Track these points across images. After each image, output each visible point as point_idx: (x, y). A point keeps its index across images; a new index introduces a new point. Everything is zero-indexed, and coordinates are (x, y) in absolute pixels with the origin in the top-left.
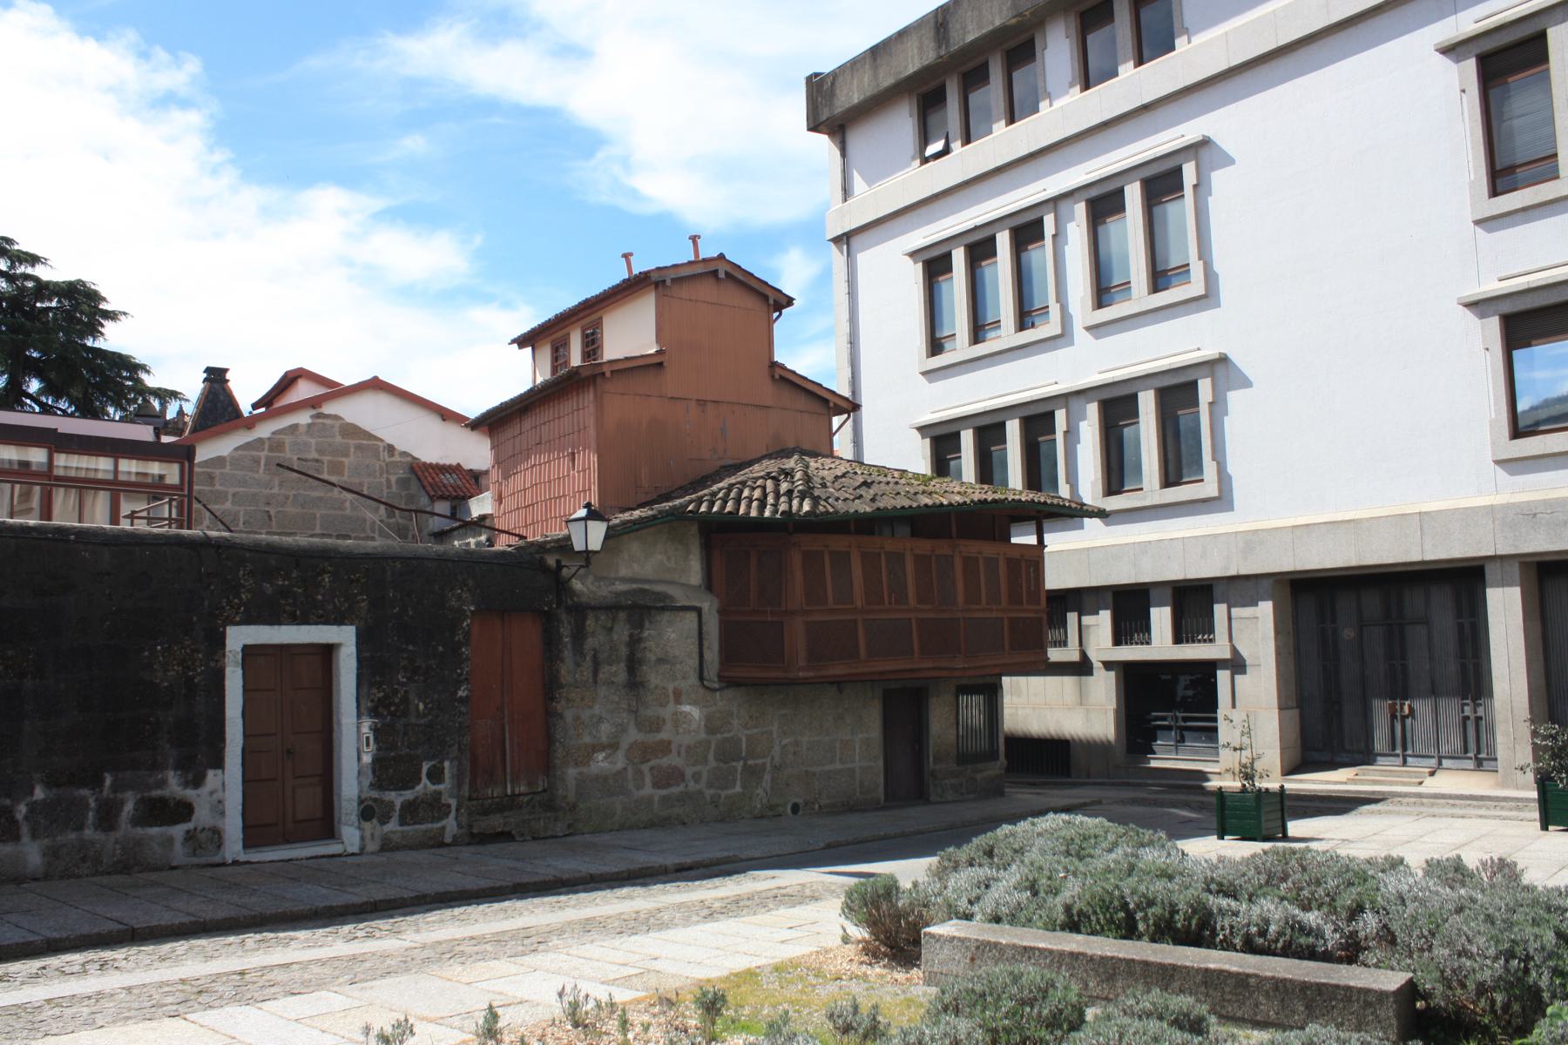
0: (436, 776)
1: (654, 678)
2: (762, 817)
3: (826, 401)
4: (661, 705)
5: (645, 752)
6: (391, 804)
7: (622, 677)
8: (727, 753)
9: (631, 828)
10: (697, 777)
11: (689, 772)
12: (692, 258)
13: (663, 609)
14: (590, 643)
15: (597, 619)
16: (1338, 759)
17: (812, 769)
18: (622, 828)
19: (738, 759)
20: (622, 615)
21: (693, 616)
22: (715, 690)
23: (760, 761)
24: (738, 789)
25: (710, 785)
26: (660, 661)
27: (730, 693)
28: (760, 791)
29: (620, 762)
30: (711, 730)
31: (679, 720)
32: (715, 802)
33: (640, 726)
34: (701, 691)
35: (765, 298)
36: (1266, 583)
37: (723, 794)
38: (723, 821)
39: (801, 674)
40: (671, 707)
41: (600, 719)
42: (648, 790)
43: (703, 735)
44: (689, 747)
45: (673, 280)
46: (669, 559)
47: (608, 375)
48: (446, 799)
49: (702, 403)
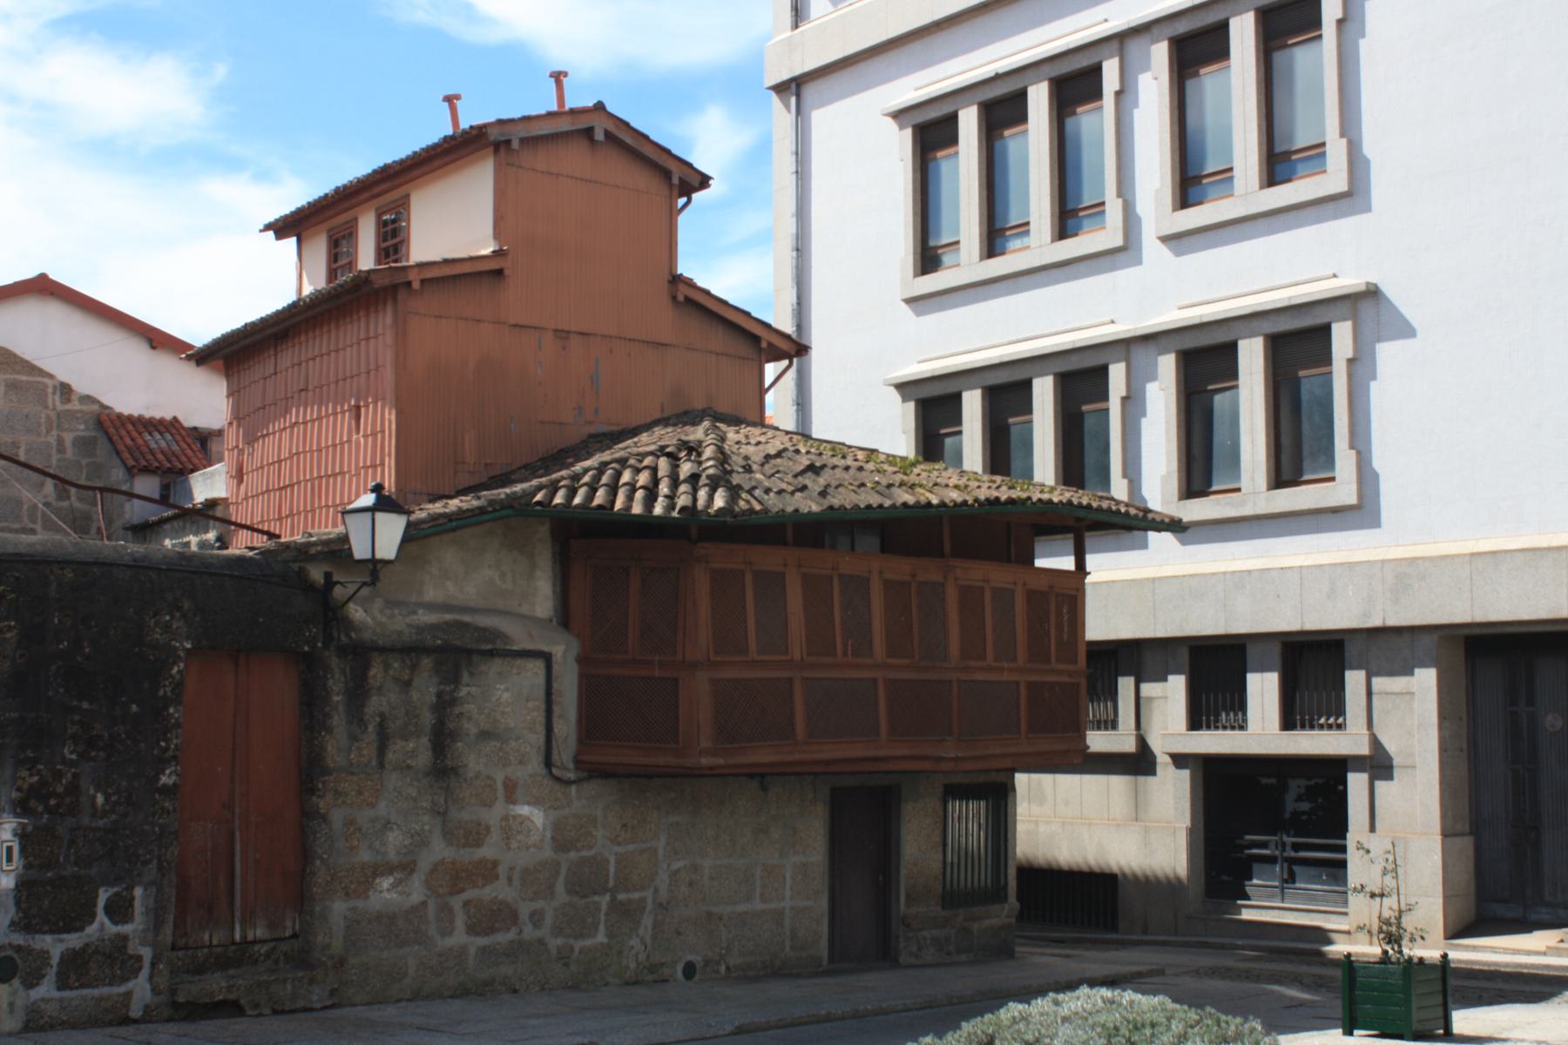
0: (119, 910)
1: (474, 761)
2: (636, 983)
3: (756, 339)
5: (456, 877)
6: (44, 956)
7: (424, 758)
8: (586, 881)
9: (430, 997)
10: (536, 918)
11: (525, 910)
12: (554, 107)
13: (492, 654)
14: (375, 704)
15: (387, 667)
16: (1534, 917)
17: (715, 910)
18: (416, 996)
20: (427, 662)
21: (538, 666)
23: (636, 895)
24: (601, 938)
25: (558, 931)
26: (485, 735)
27: (593, 787)
28: (634, 942)
29: (416, 892)
30: (562, 842)
31: (511, 828)
32: (564, 957)
33: (448, 835)
34: (547, 782)
35: (666, 174)
36: (1428, 641)
37: (578, 945)
38: (575, 987)
39: (704, 761)
40: (499, 808)
41: (387, 825)
42: (459, 937)
43: (548, 853)
44: (526, 871)
45: (523, 141)
46: (503, 575)
47: (416, 285)
48: (134, 948)
49: (562, 335)
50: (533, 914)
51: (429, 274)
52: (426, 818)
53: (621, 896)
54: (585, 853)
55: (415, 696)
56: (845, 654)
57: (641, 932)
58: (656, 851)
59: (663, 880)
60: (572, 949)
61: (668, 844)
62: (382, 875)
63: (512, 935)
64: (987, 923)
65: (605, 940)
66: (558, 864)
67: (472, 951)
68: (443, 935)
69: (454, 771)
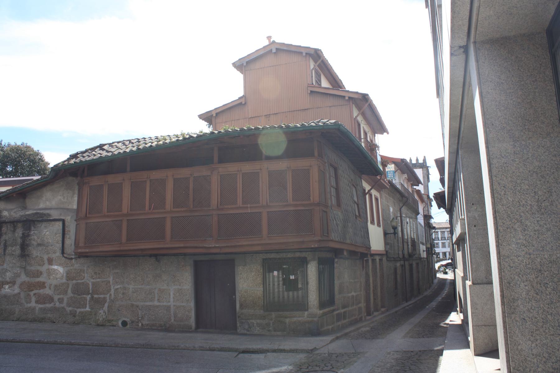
1: (35, 252)
2: (102, 325)
4: (40, 265)
5: (29, 287)
7: (18, 251)
9: (22, 320)
10: (61, 301)
11: (56, 298)
18: (18, 320)
19: (88, 294)
20: (20, 225)
21: (60, 224)
22: (72, 259)
23: (102, 296)
24: (88, 309)
25: (69, 305)
26: (39, 245)
27: (82, 260)
28: (101, 311)
30: (69, 277)
31: (50, 273)
32: (73, 314)
33: (27, 274)
34: (63, 258)
37: (78, 310)
40: (46, 266)
41: (6, 270)
42: (33, 304)
43: (64, 280)
44: (56, 286)
46: (64, 198)
49: (267, 116)
50: (59, 299)
51: (218, 111)
52: (18, 269)
53: (95, 296)
54: (79, 281)
55: (16, 235)
56: (150, 209)
57: (104, 309)
58: (109, 282)
59: (112, 292)
60: (76, 311)
61: (113, 279)
62: (5, 284)
63: (52, 305)
64: (295, 319)
65: (89, 310)
66: (68, 284)
67: (37, 309)
68: (27, 303)
69: (28, 255)
